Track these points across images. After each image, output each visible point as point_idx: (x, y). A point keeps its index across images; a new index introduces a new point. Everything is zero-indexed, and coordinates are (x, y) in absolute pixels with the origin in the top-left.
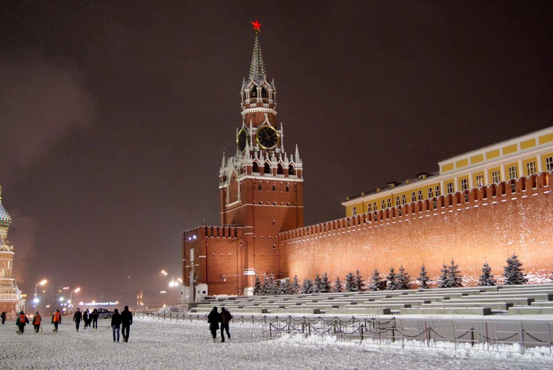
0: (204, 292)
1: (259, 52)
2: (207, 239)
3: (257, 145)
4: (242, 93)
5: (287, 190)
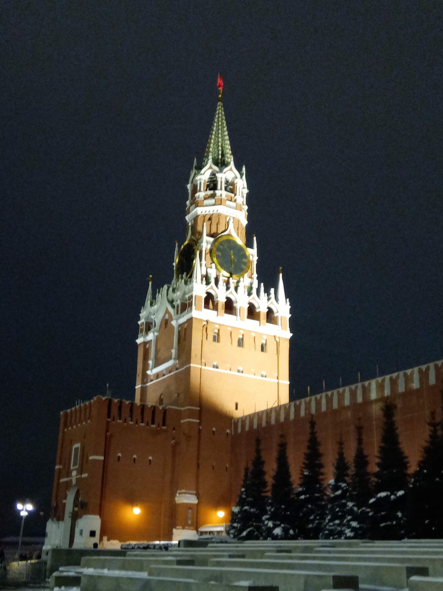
0: (93, 534)
1: (222, 119)
3: (213, 265)
4: (189, 186)
5: (263, 348)
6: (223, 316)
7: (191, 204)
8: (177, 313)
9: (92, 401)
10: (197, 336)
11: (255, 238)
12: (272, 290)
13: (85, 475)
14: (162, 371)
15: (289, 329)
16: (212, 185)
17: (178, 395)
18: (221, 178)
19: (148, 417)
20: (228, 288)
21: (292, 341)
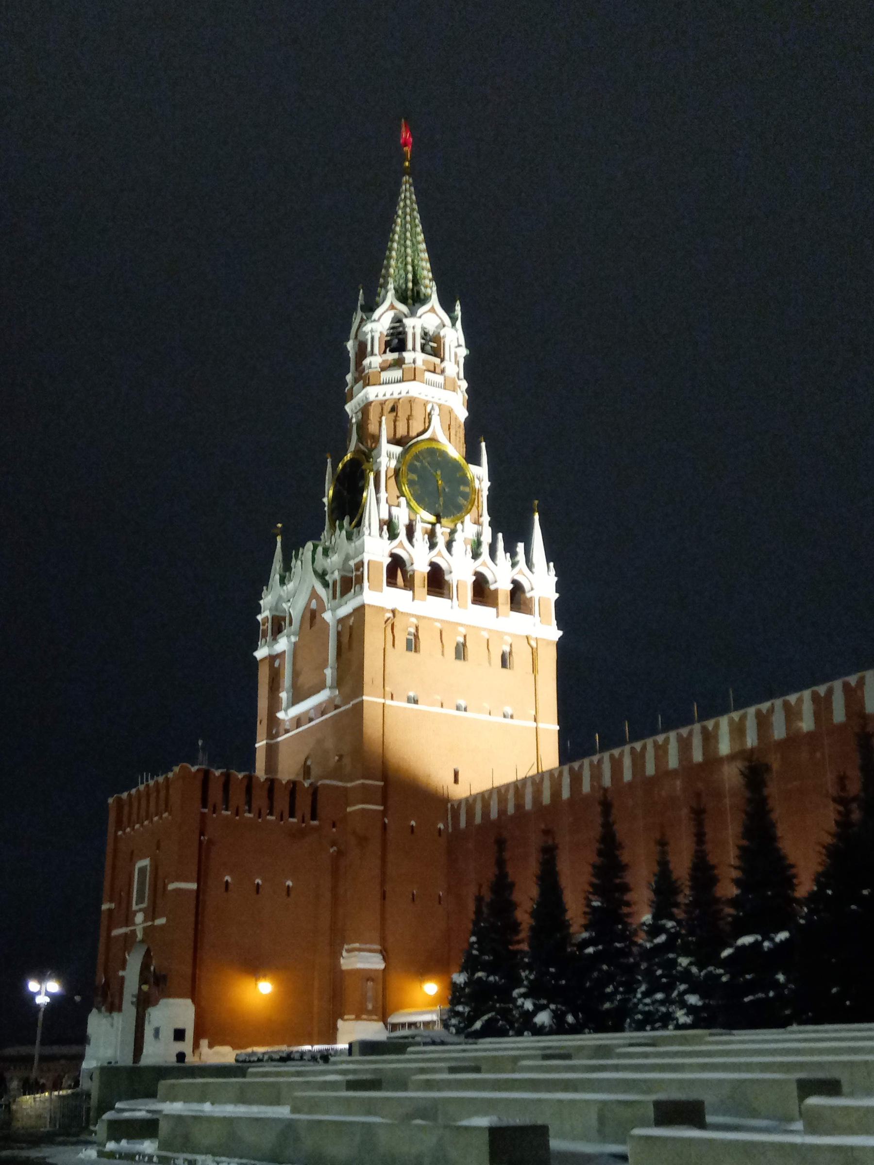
0: (179, 1035)
1: (413, 210)
2: (203, 815)
3: (403, 500)
4: (350, 345)
5: (505, 661)
6: (424, 600)
7: (356, 381)
8: (334, 597)
9: (170, 775)
10: (373, 640)
11: (483, 444)
12: (520, 547)
13: (161, 921)
14: (307, 712)
15: (555, 622)
16: (397, 341)
17: (341, 757)
18: (414, 328)
19: (282, 802)
20: (433, 546)
21: (562, 646)
